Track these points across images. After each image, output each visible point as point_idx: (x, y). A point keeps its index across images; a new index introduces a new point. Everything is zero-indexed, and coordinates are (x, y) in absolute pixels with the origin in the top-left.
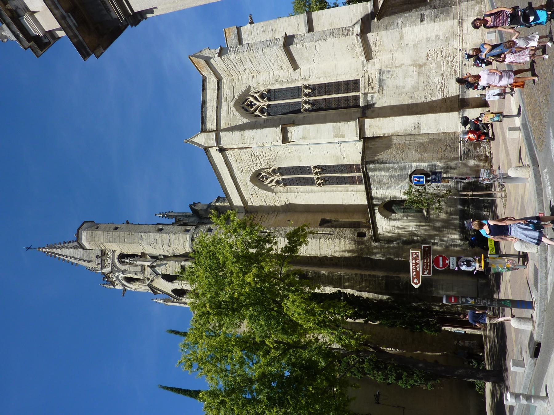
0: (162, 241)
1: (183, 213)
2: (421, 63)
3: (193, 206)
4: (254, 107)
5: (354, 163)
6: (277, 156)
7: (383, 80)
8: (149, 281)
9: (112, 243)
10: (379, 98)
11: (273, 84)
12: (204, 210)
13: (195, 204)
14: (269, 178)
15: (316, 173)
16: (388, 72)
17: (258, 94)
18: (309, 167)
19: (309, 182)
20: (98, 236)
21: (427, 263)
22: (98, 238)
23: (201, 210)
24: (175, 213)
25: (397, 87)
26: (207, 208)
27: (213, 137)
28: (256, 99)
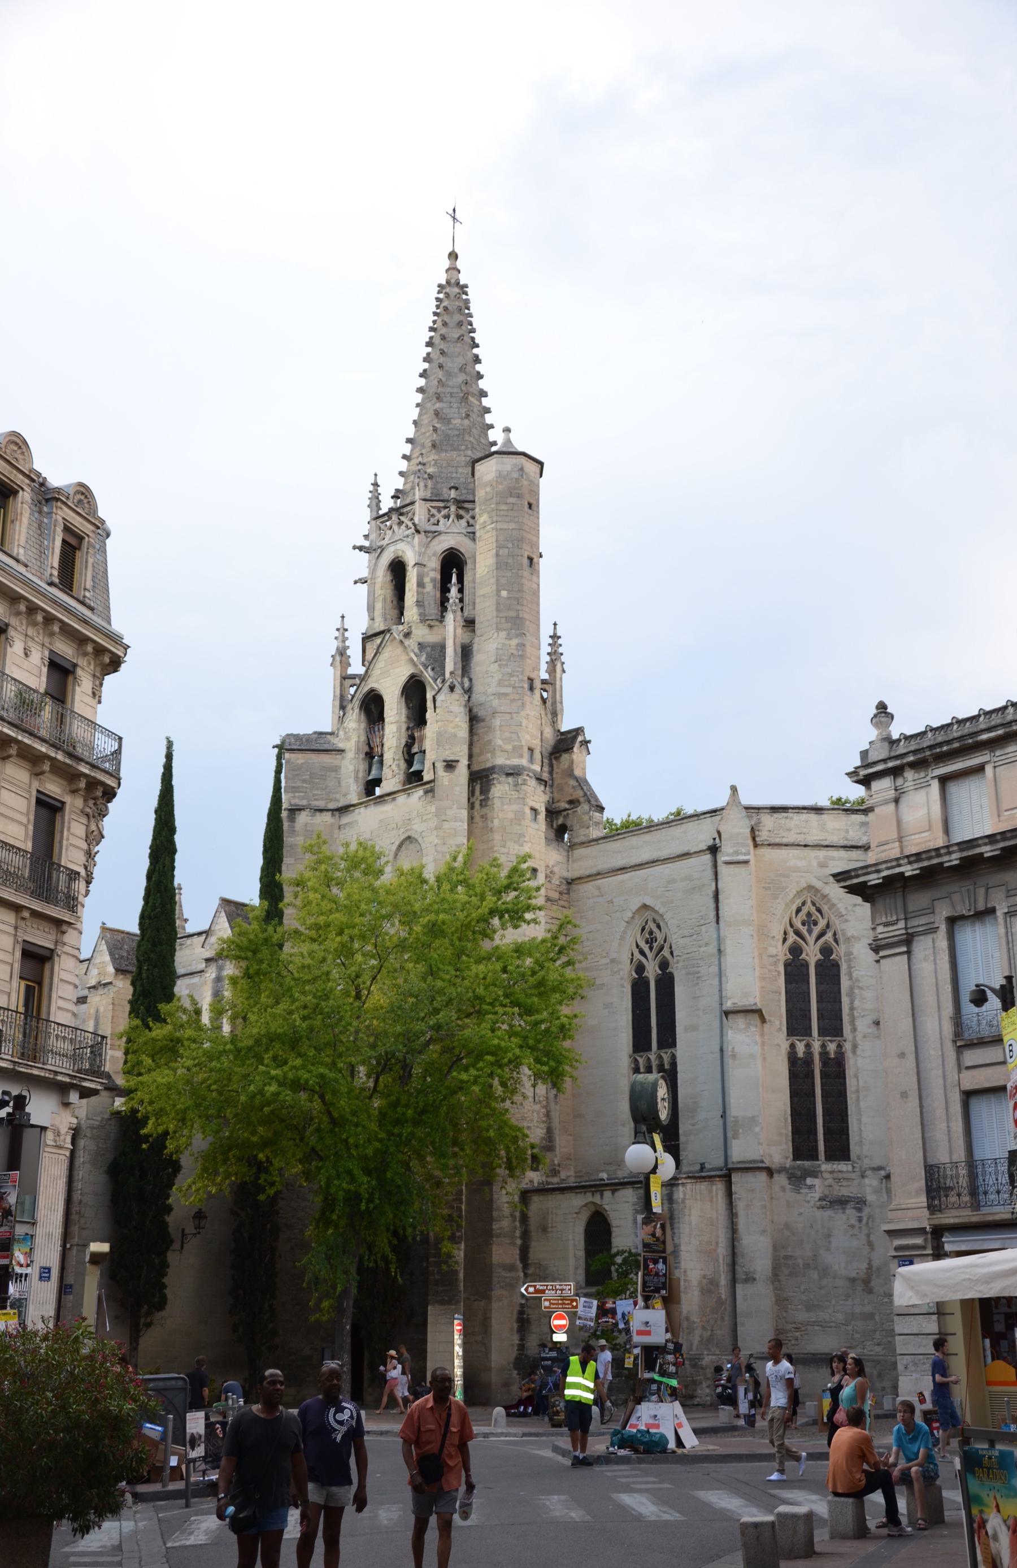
0: (506, 695)
1: (561, 703)
2: (873, 1283)
3: (580, 738)
4: (804, 930)
5: (681, 1146)
6: (698, 978)
7: (844, 1209)
8: (402, 637)
9: (497, 555)
10: (808, 1202)
11: (851, 978)
13: (586, 743)
14: (651, 948)
15: (660, 1057)
16: (860, 1220)
17: (831, 940)
18: (673, 1044)
19: (640, 1042)
20: (510, 513)
21: (558, 1304)
22: (505, 513)
23: (572, 762)
24: (561, 679)
25: (829, 1236)
26: (577, 779)
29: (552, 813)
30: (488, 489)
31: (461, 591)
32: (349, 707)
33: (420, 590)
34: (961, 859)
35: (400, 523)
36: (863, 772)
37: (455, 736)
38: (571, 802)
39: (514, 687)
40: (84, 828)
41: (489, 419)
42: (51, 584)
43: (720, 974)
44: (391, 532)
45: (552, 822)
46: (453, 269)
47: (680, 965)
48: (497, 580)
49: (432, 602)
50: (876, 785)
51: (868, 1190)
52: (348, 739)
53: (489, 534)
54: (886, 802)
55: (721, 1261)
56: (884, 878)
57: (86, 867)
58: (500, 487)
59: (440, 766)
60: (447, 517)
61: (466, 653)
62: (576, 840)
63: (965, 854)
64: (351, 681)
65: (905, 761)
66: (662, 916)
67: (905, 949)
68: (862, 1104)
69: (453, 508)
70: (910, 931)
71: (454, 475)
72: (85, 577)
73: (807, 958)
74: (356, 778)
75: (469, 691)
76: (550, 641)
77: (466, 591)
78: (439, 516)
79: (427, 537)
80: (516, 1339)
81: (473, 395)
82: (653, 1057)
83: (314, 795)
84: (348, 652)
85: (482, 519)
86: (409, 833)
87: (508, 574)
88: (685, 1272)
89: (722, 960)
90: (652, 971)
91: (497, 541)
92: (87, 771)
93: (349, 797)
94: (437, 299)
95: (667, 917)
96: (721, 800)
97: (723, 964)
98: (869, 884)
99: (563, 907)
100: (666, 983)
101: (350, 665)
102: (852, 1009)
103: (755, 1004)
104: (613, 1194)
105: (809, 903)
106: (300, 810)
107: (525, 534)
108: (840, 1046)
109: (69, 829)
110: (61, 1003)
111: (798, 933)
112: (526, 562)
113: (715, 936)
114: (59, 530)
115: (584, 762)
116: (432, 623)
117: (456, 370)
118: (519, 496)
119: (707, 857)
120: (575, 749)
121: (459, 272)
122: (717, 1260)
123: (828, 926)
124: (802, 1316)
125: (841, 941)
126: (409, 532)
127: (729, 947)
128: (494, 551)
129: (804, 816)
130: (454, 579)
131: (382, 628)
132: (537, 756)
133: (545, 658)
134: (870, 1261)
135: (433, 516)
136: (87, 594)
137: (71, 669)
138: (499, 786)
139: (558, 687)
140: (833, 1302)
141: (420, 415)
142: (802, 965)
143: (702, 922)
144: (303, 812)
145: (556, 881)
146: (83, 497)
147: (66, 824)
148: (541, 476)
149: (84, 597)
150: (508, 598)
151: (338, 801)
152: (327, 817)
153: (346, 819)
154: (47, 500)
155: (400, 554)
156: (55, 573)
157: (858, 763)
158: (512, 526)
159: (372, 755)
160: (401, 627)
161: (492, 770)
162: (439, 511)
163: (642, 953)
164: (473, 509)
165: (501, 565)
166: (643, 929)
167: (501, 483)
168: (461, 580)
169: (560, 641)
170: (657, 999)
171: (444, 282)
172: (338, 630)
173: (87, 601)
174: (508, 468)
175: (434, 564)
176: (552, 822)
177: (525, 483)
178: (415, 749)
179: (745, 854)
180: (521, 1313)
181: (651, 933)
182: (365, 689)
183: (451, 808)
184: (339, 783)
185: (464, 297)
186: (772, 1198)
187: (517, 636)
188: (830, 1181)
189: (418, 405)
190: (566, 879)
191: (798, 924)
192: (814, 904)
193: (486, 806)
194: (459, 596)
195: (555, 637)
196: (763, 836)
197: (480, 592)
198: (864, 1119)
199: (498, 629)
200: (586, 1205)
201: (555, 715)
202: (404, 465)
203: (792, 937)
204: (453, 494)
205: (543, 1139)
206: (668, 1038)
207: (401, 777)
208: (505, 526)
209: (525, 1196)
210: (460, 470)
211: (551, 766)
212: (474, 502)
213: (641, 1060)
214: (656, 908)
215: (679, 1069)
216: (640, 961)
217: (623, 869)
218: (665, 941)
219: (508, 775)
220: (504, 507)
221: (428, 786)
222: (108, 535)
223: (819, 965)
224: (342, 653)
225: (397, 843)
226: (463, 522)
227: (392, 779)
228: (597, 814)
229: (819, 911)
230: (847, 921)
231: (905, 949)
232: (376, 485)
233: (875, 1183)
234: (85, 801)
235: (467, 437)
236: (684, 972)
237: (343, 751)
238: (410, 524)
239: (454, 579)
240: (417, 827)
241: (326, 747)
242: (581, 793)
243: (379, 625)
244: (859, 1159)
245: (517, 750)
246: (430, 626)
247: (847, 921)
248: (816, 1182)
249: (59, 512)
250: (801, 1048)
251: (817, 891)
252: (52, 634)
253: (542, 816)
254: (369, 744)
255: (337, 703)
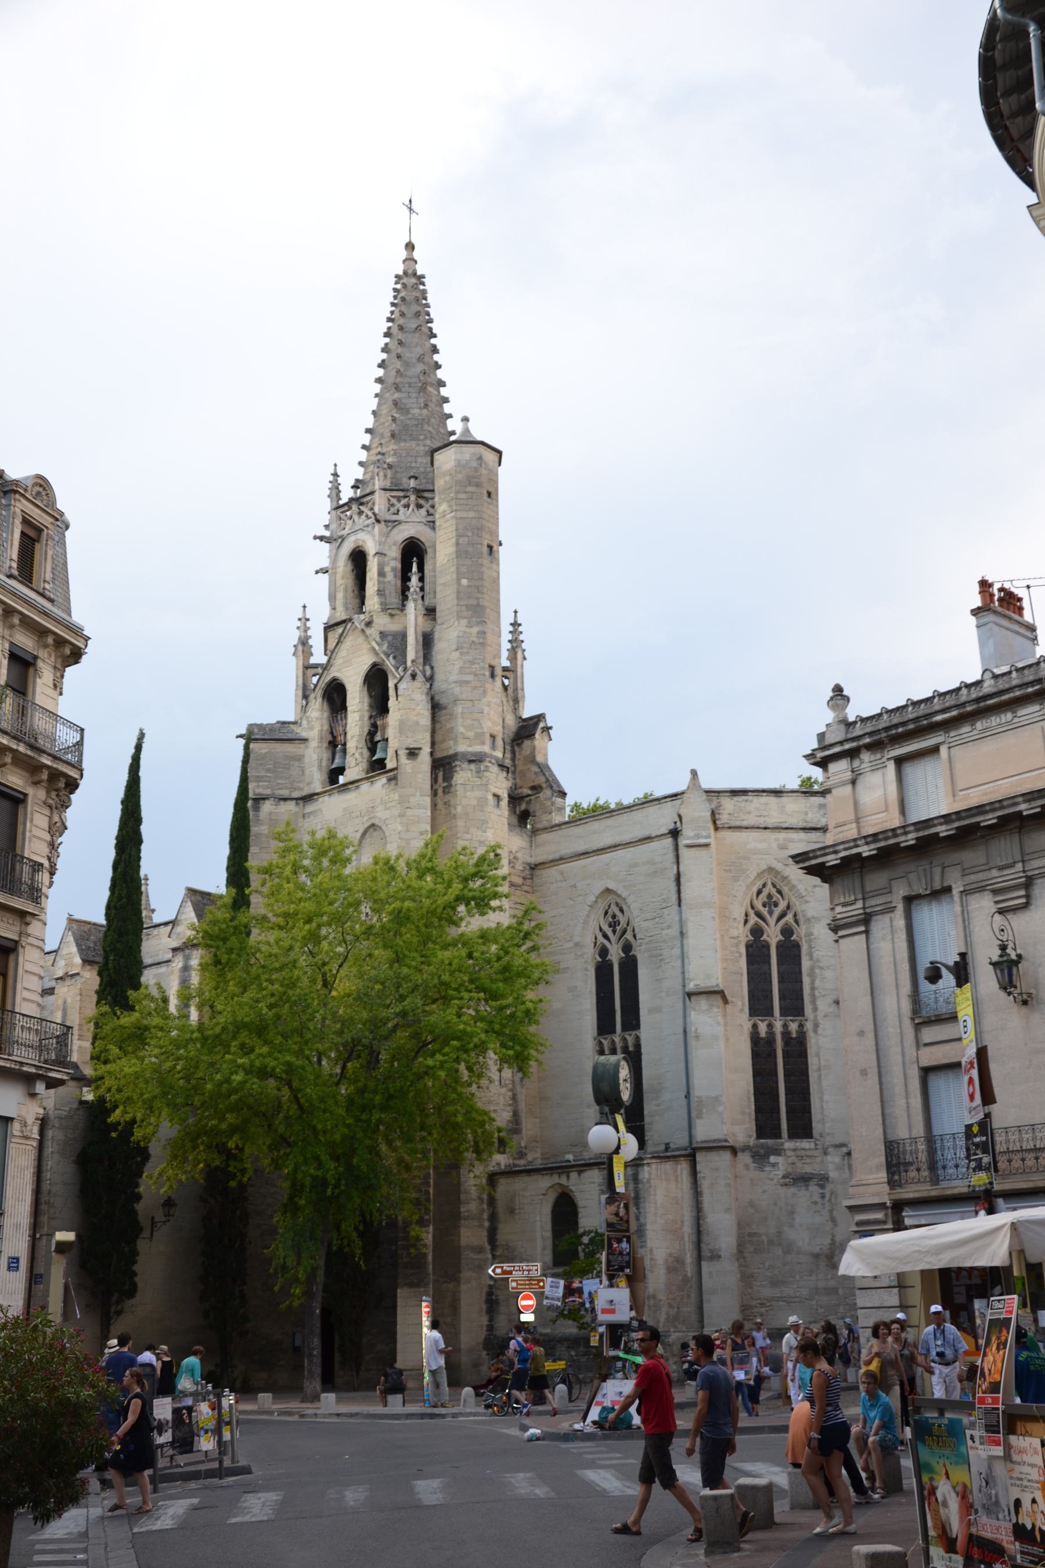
0: (467, 682)
1: (523, 689)
3: (542, 725)
4: (765, 911)
5: (646, 1127)
7: (807, 1186)
8: (363, 626)
9: (457, 544)
10: (772, 1179)
11: (811, 958)
12: (534, 757)
13: (547, 729)
14: (614, 932)
15: (624, 1040)
16: (823, 1196)
17: (792, 921)
18: (637, 1026)
19: (605, 1026)
20: (470, 502)
22: (465, 502)
23: (534, 748)
26: (539, 765)
27: (702, 837)
28: (782, 915)
29: (514, 799)
30: (448, 478)
31: (421, 579)
32: (312, 696)
33: (381, 579)
34: (917, 839)
35: (361, 513)
36: (820, 755)
37: (417, 723)
38: (533, 788)
39: (475, 675)
40: (47, 819)
41: (447, 408)
42: (10, 576)
43: (683, 957)
44: (351, 522)
45: (515, 808)
46: (410, 260)
47: (643, 947)
48: (458, 568)
49: (393, 591)
50: (833, 767)
51: (831, 1167)
52: (311, 728)
53: (449, 523)
54: (843, 784)
55: (686, 1239)
56: (842, 858)
57: (49, 859)
58: (459, 476)
59: (403, 753)
60: (407, 506)
61: (427, 641)
62: (539, 826)
63: (921, 834)
64: (314, 671)
65: (861, 743)
66: (624, 899)
67: (863, 928)
68: (825, 1083)
69: (413, 498)
70: (868, 911)
71: (414, 465)
72: (44, 570)
73: (768, 939)
74: (320, 766)
75: (430, 679)
76: (511, 629)
77: (427, 579)
78: (398, 505)
79: (387, 526)
80: (485, 1320)
81: (432, 385)
82: (617, 1039)
83: (278, 784)
84: (311, 642)
85: (442, 508)
86: (373, 821)
87: (468, 562)
88: (651, 1251)
89: (685, 942)
90: (615, 954)
91: (457, 529)
92: (49, 763)
93: (312, 786)
94: (395, 290)
95: (630, 900)
96: (681, 784)
97: (685, 946)
98: (828, 864)
99: (527, 892)
100: (630, 966)
101: (312, 655)
102: (813, 989)
103: (718, 985)
104: (579, 1174)
105: (769, 885)
106: (264, 799)
107: (485, 523)
108: (801, 1026)
109: (32, 820)
110: (26, 994)
111: (759, 915)
112: (485, 550)
113: (677, 918)
114: (18, 522)
115: (546, 748)
116: (393, 612)
117: (414, 360)
118: (478, 485)
119: (669, 841)
120: (537, 736)
121: (416, 262)
122: (683, 1238)
123: (788, 907)
124: (767, 1292)
125: (801, 921)
126: (369, 522)
127: (691, 929)
128: (454, 540)
129: (764, 799)
130: (415, 568)
131: (344, 617)
132: (499, 743)
133: (506, 646)
134: (833, 1236)
135: (393, 505)
136: (47, 586)
137: (31, 661)
138: (461, 773)
139: (519, 674)
140: (798, 1277)
141: (379, 405)
142: (763, 946)
143: (664, 905)
144: (267, 802)
145: (519, 867)
146: (41, 489)
147: (29, 816)
148: (500, 465)
149: (44, 589)
150: (469, 586)
151: (302, 789)
152: (291, 806)
153: (310, 808)
154: (5, 493)
155: (360, 543)
156: (15, 565)
157: (816, 746)
158: (471, 514)
159: (335, 744)
160: (362, 617)
161: (454, 757)
162: (399, 501)
163: (606, 936)
164: (433, 499)
165: (461, 553)
166: (606, 913)
167: (460, 472)
168: (421, 569)
169: (520, 629)
170: (620, 981)
171: (401, 273)
172: (300, 619)
173: (47, 593)
174: (467, 457)
175: (394, 554)
176: (515, 808)
177: (484, 472)
178: (378, 738)
179: (706, 837)
180: (490, 1294)
181: (614, 916)
182: (328, 678)
183: (414, 795)
184: (303, 772)
185: (421, 287)
186: (736, 1177)
187: (478, 624)
188: (793, 1159)
189: (377, 395)
190: (529, 864)
191: (760, 907)
192: (774, 886)
193: (449, 792)
194: (420, 585)
195: (515, 624)
196: (723, 819)
197: (441, 580)
198: (826, 1098)
199: (459, 617)
200: (552, 1187)
201: (516, 701)
202: (363, 456)
203: (753, 919)
204: (412, 483)
205: (509, 1121)
206: (632, 1021)
207: (364, 765)
208: (465, 515)
209: (493, 1178)
210: (419, 460)
211: (513, 752)
212: (433, 491)
213: (605, 1043)
214: (619, 892)
215: (643, 1050)
216: (604, 945)
217: (585, 854)
218: (628, 925)
219: (470, 761)
220: (463, 496)
221: (391, 774)
222: (67, 527)
223: (780, 946)
224: (304, 643)
225: (361, 831)
226: (423, 512)
227: (355, 767)
228: (559, 800)
229: (780, 892)
230: (807, 902)
231: (863, 928)
232: (336, 475)
233: (837, 1160)
234: (48, 792)
235: (426, 427)
236: (647, 954)
237: (306, 740)
238: (370, 514)
239: (415, 568)
240: (381, 815)
241: (289, 736)
242: (542, 779)
243: (341, 615)
244: (821, 1135)
245: (479, 738)
246: (392, 615)
247: (807, 902)
248: (779, 1160)
249: (18, 504)
250: (763, 1028)
251: (777, 873)
252: (12, 627)
253: (505, 802)
254: (332, 733)
255: (300, 693)
